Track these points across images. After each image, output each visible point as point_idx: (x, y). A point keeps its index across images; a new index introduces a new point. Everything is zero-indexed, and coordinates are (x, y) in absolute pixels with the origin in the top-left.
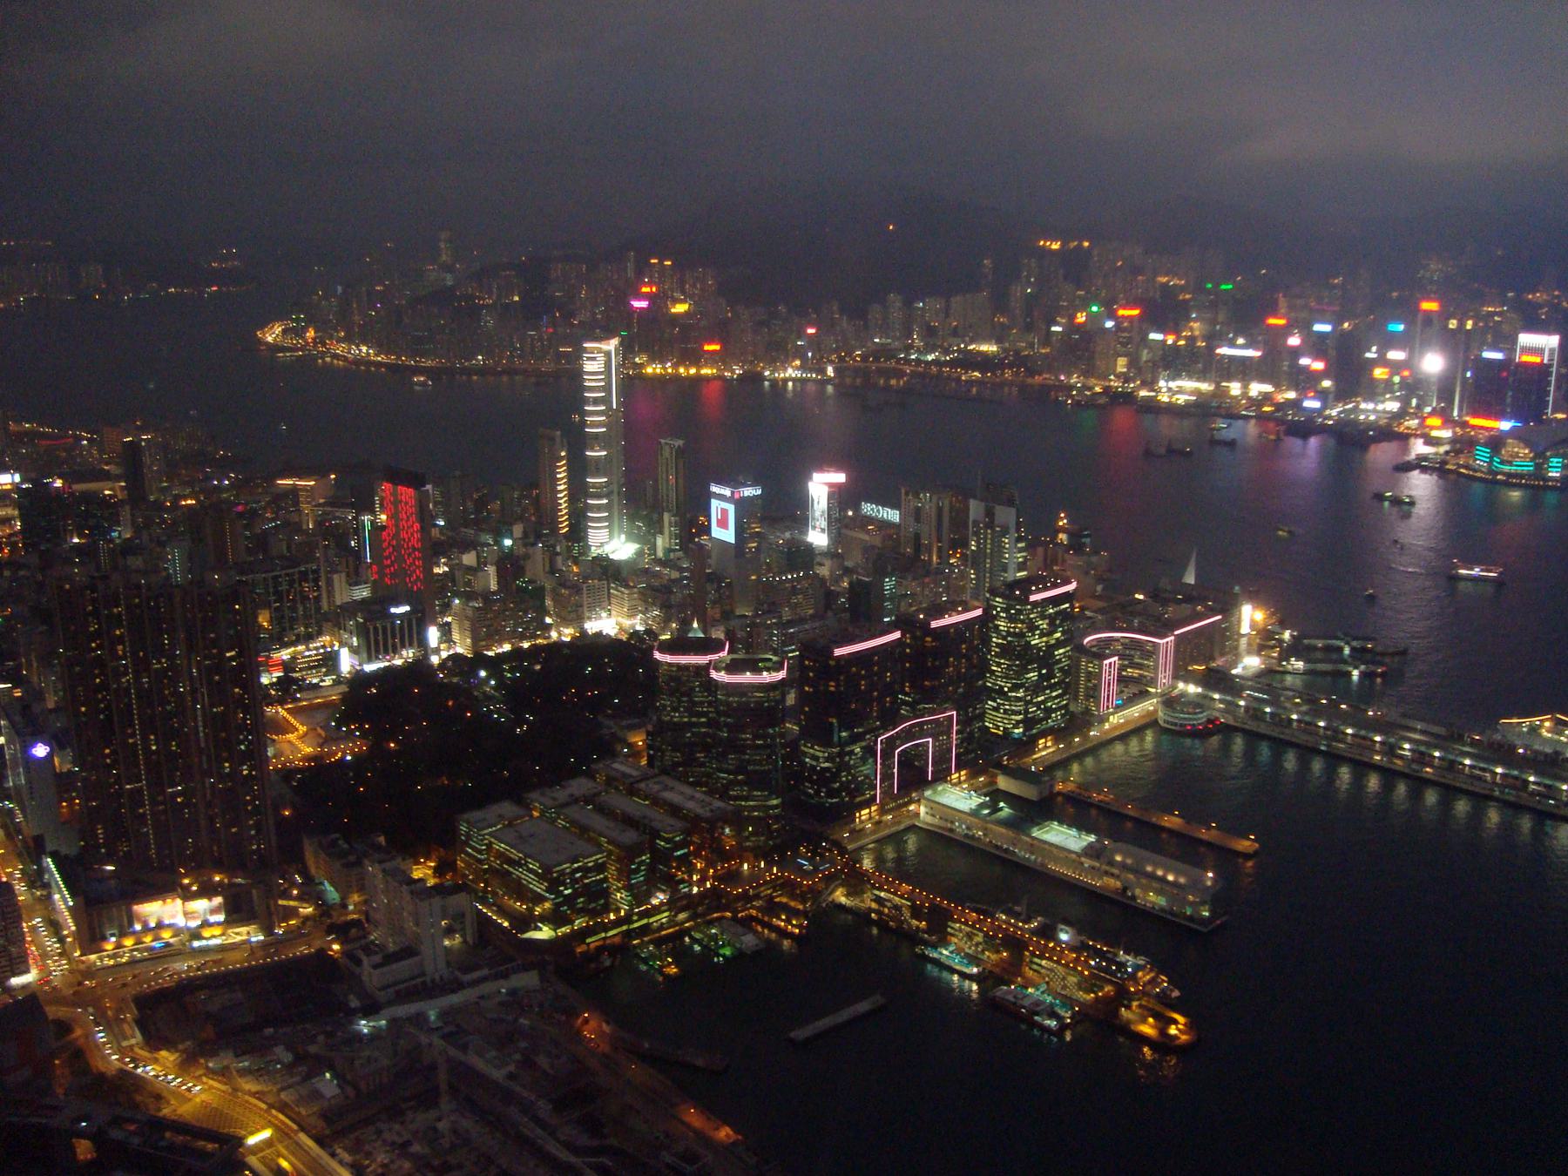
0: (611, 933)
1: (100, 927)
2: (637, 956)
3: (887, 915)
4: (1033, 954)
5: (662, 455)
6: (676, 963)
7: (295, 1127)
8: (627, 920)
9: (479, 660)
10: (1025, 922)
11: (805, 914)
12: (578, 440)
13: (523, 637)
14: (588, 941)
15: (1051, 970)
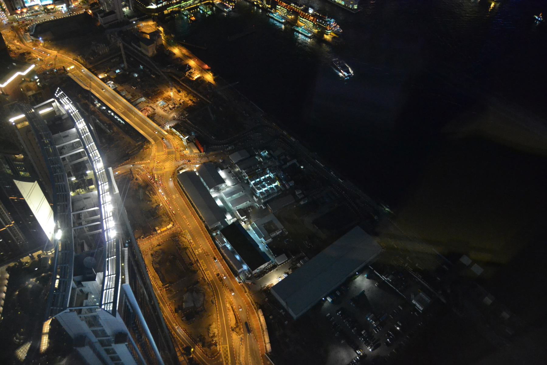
3: (259, 3)
4: (301, 17)
6: (194, 16)
7: (81, 65)
10: (299, 7)
14: (168, 9)
15: (306, 22)
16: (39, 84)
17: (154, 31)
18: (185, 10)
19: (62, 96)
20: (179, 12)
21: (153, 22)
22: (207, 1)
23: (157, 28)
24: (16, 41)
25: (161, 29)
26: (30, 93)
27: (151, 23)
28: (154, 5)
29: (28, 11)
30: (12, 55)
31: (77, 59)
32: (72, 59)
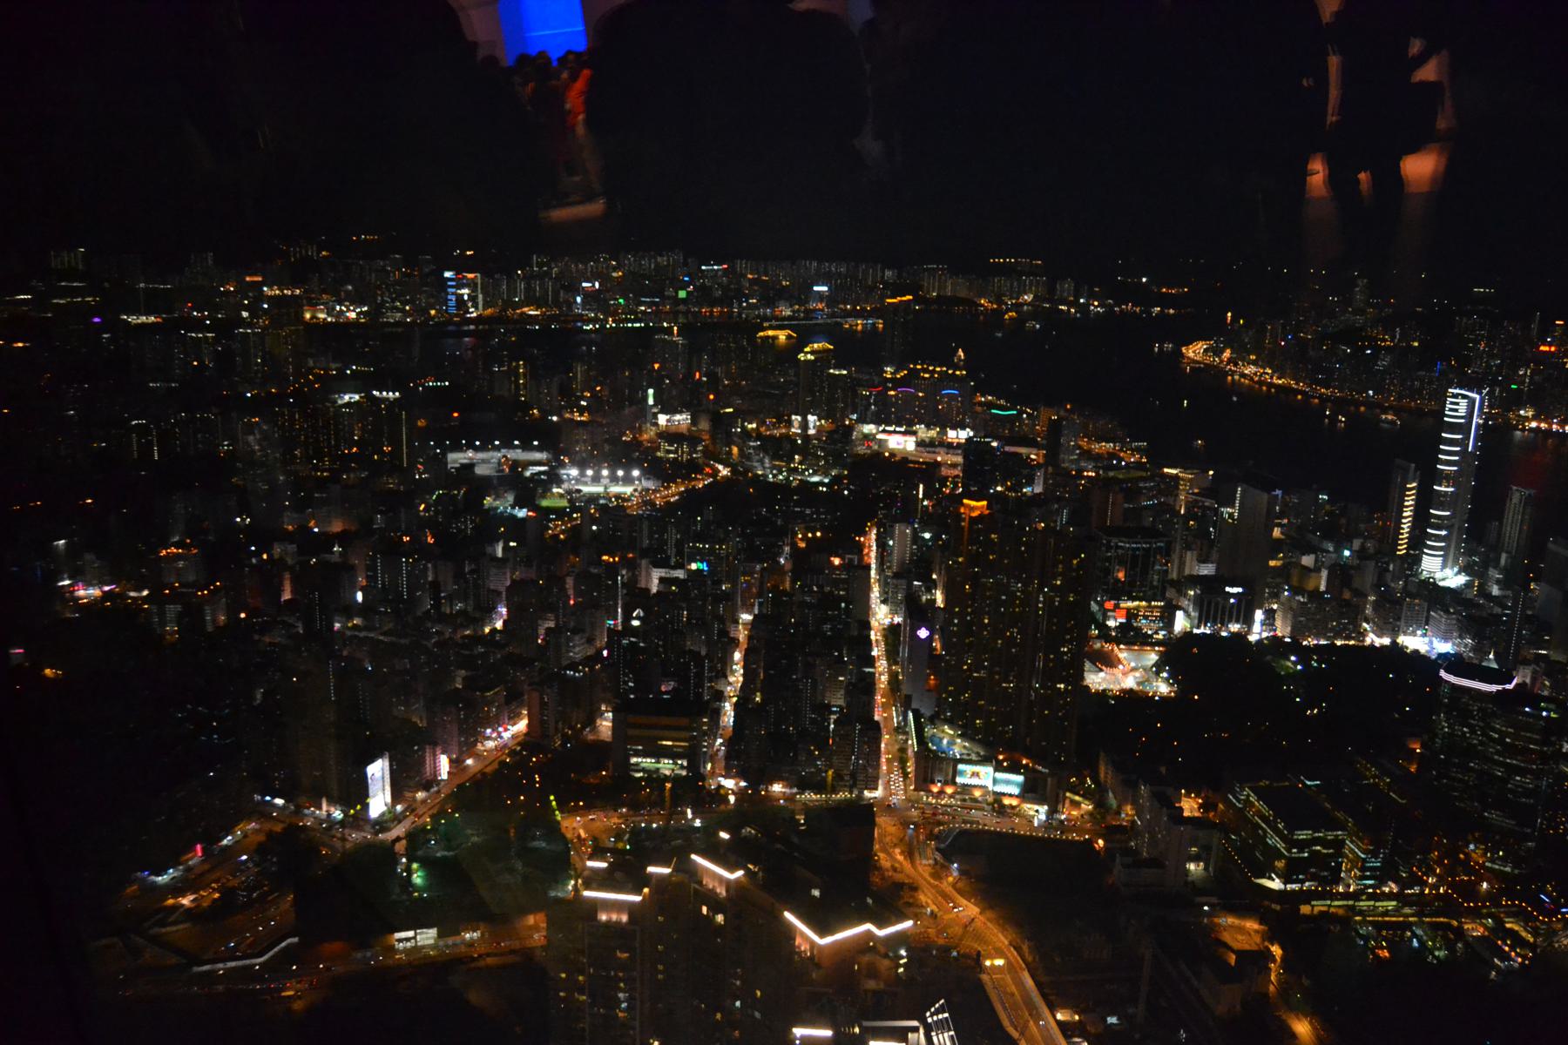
0: (1336, 903)
1: (932, 774)
2: (1357, 933)
5: (1511, 500)
6: (1388, 948)
7: (1023, 965)
8: (1356, 896)
9: (1295, 647)
11: (1533, 947)
12: (1430, 476)
13: (1338, 635)
14: (1313, 903)
16: (901, 970)
17: (1253, 949)
18: (1364, 923)
19: (941, 1026)
20: (1345, 921)
21: (1261, 924)
22: (1442, 919)
23: (1266, 943)
24: (897, 851)
25: (1276, 950)
26: (871, 985)
27: (1252, 925)
28: (1277, 880)
29: (955, 793)
30: (876, 879)
31: (1020, 947)
32: (1006, 942)
